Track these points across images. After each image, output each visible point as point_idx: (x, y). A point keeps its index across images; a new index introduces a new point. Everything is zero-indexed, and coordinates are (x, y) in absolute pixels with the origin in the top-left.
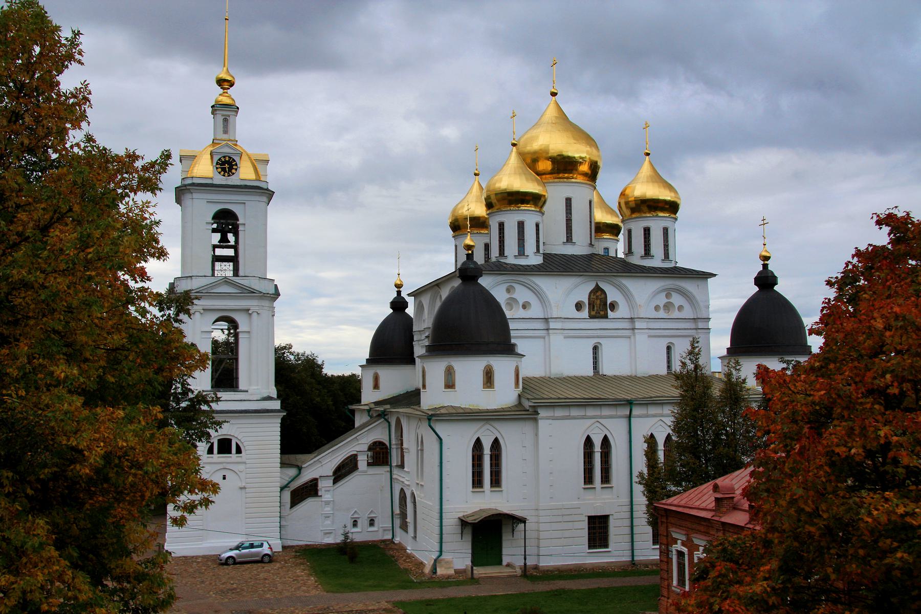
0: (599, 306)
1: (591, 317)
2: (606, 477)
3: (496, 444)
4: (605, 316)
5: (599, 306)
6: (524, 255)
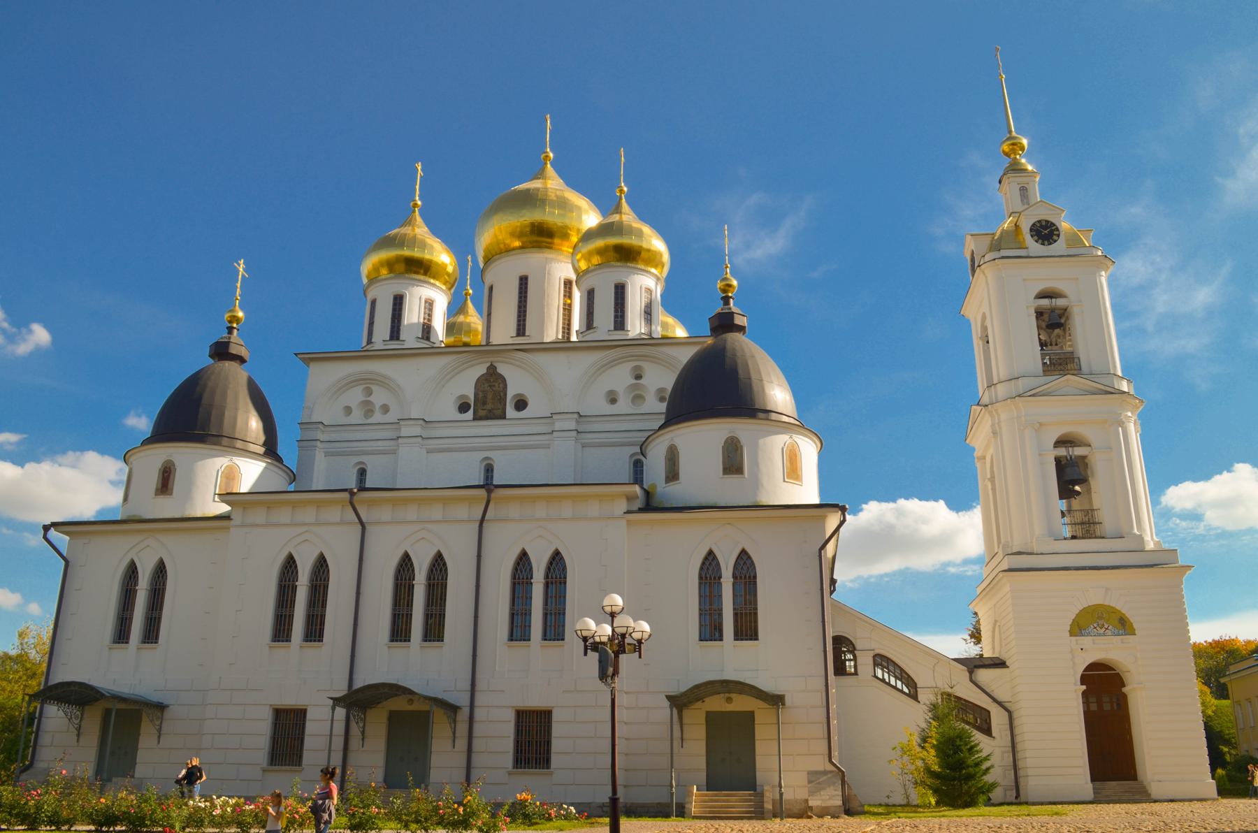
0: (490, 400)
1: (474, 419)
2: (315, 631)
3: (160, 571)
4: (503, 416)
5: (490, 400)
6: (398, 339)
